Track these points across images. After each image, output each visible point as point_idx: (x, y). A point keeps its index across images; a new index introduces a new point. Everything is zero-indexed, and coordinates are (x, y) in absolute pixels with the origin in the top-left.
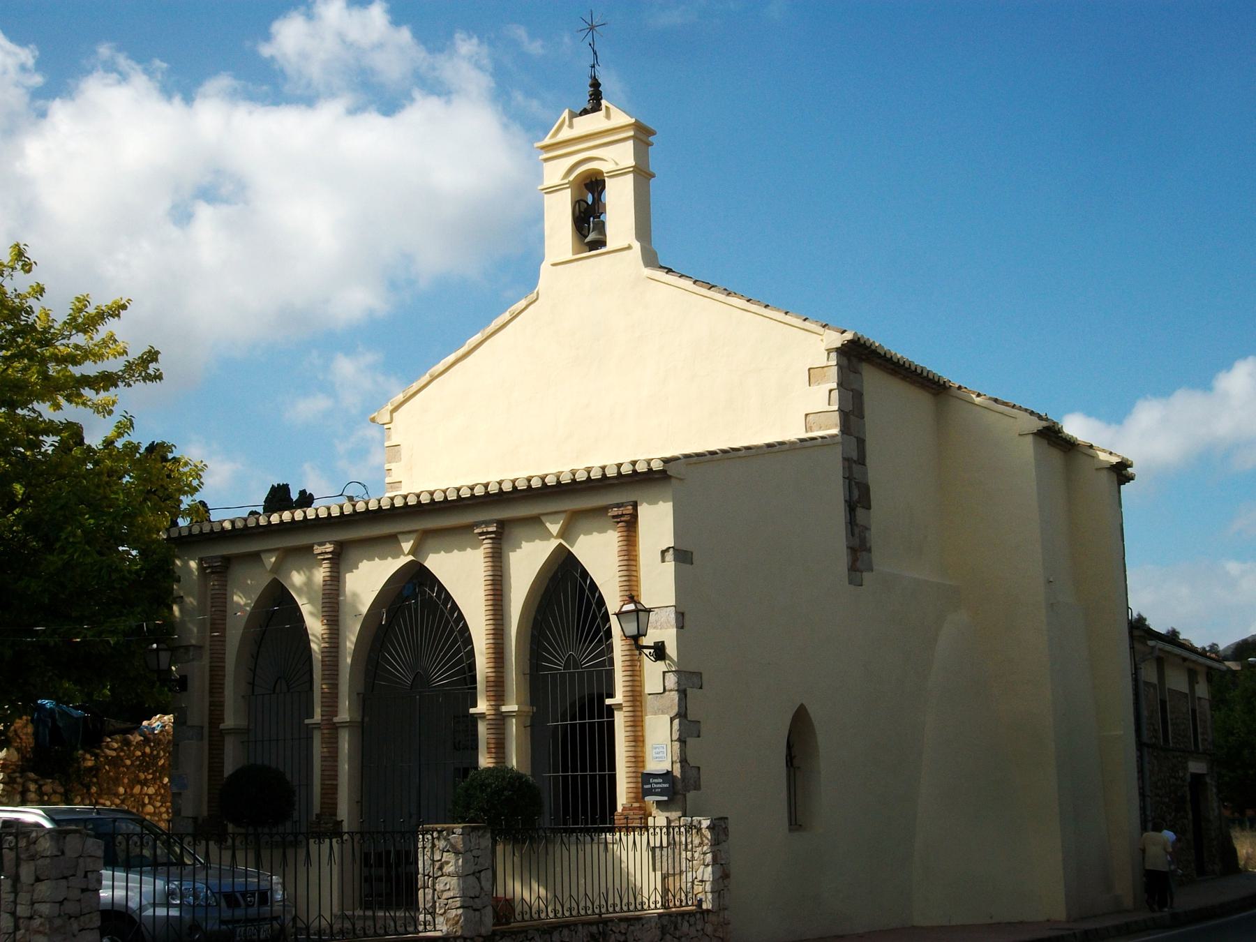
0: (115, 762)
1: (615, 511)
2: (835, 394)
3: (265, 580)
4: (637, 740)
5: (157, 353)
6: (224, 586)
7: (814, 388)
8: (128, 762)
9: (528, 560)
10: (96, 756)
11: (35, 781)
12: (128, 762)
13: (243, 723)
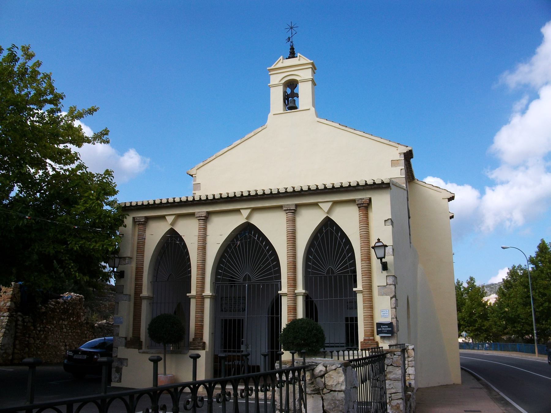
0: (53, 310)
1: (360, 202)
2: (403, 171)
3: (168, 228)
4: (370, 307)
5: (108, 131)
6: (144, 231)
7: (394, 168)
8: (58, 311)
9: (308, 222)
10: (46, 307)
11: (21, 316)
12: (58, 311)
13: (151, 295)
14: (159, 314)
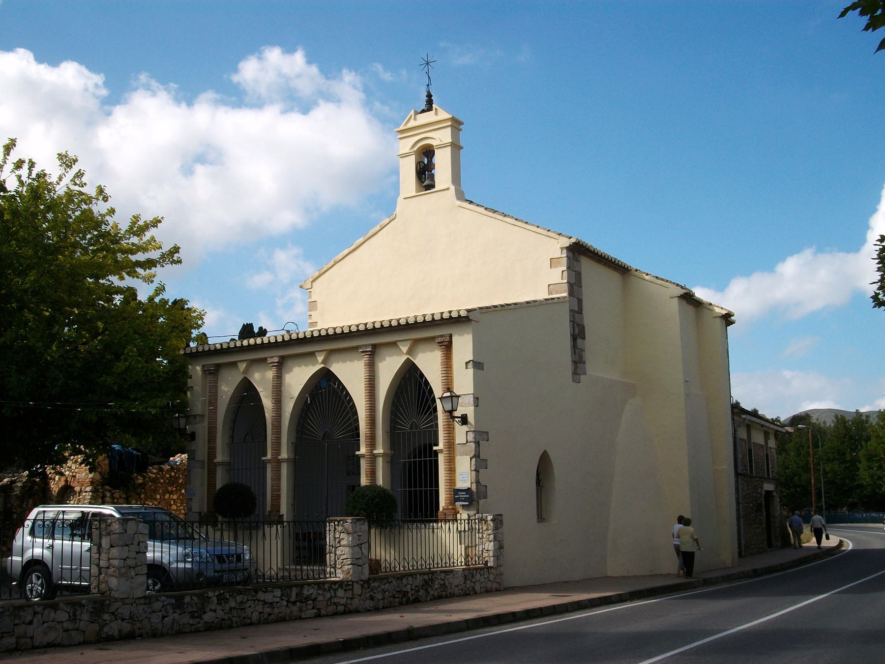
0: (155, 481)
1: (440, 340)
2: (565, 273)
3: (239, 378)
4: (451, 470)
5: (179, 248)
6: (216, 382)
7: (554, 269)
8: (162, 481)
9: (389, 367)
10: (144, 477)
11: (110, 491)
12: (162, 481)
13: (227, 459)
14: (236, 482)
